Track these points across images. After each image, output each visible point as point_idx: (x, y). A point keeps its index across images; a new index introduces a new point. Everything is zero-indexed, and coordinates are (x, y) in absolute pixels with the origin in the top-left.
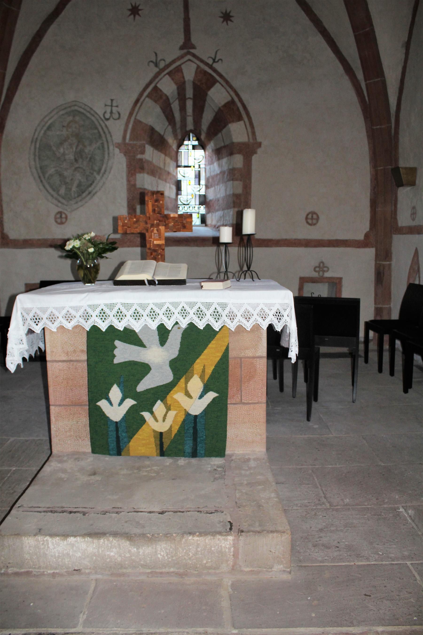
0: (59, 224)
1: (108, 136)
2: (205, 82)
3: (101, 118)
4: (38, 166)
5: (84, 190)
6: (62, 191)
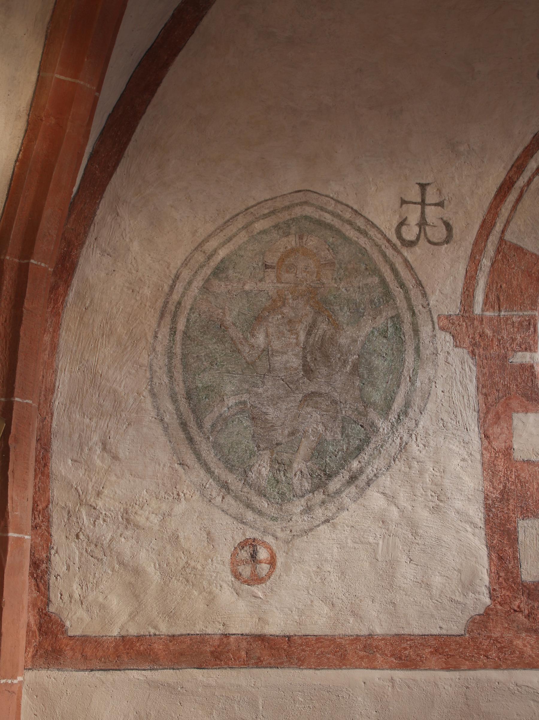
0: (246, 582)
1: (414, 293)
3: (389, 241)
4: (180, 389)
5: (334, 469)
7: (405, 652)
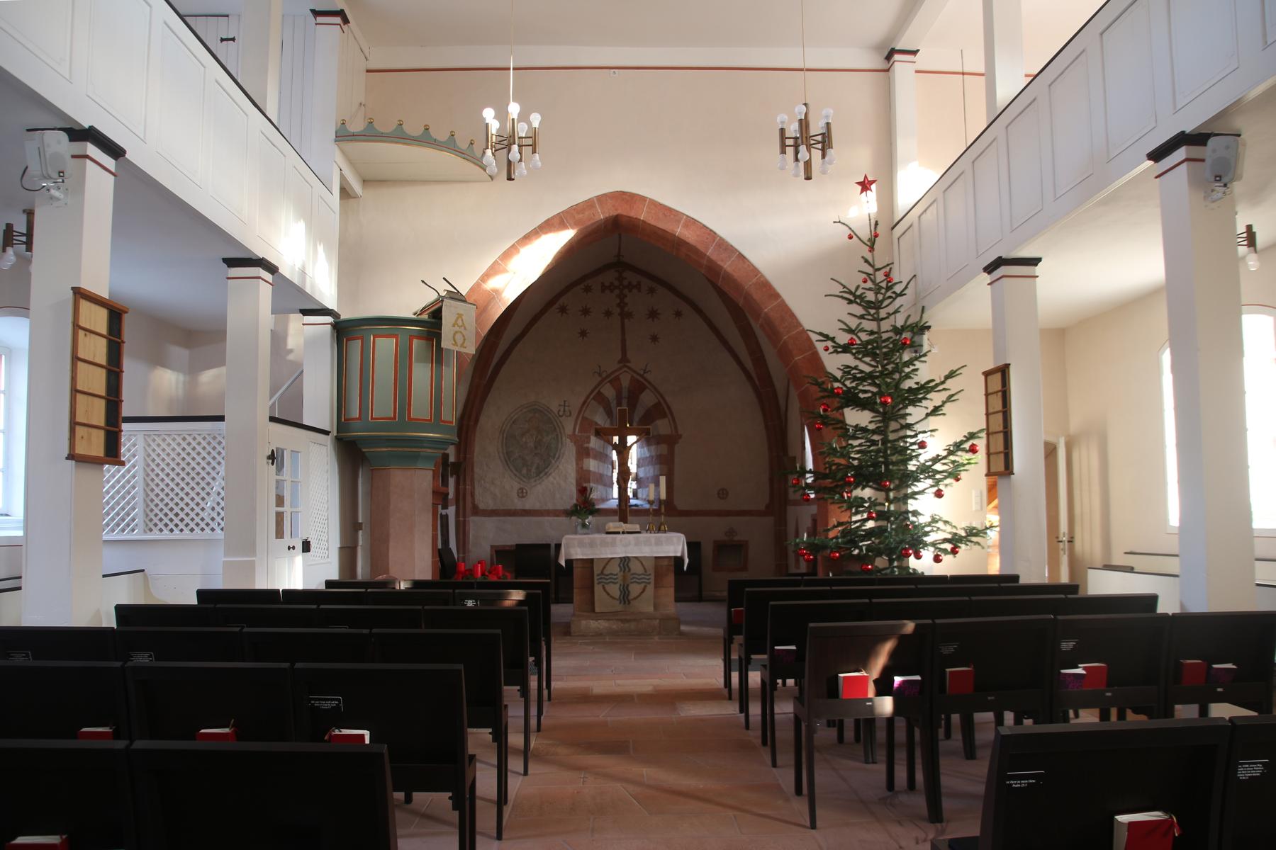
2: (638, 387)
5: (542, 471)
6: (524, 471)
7: (556, 513)
